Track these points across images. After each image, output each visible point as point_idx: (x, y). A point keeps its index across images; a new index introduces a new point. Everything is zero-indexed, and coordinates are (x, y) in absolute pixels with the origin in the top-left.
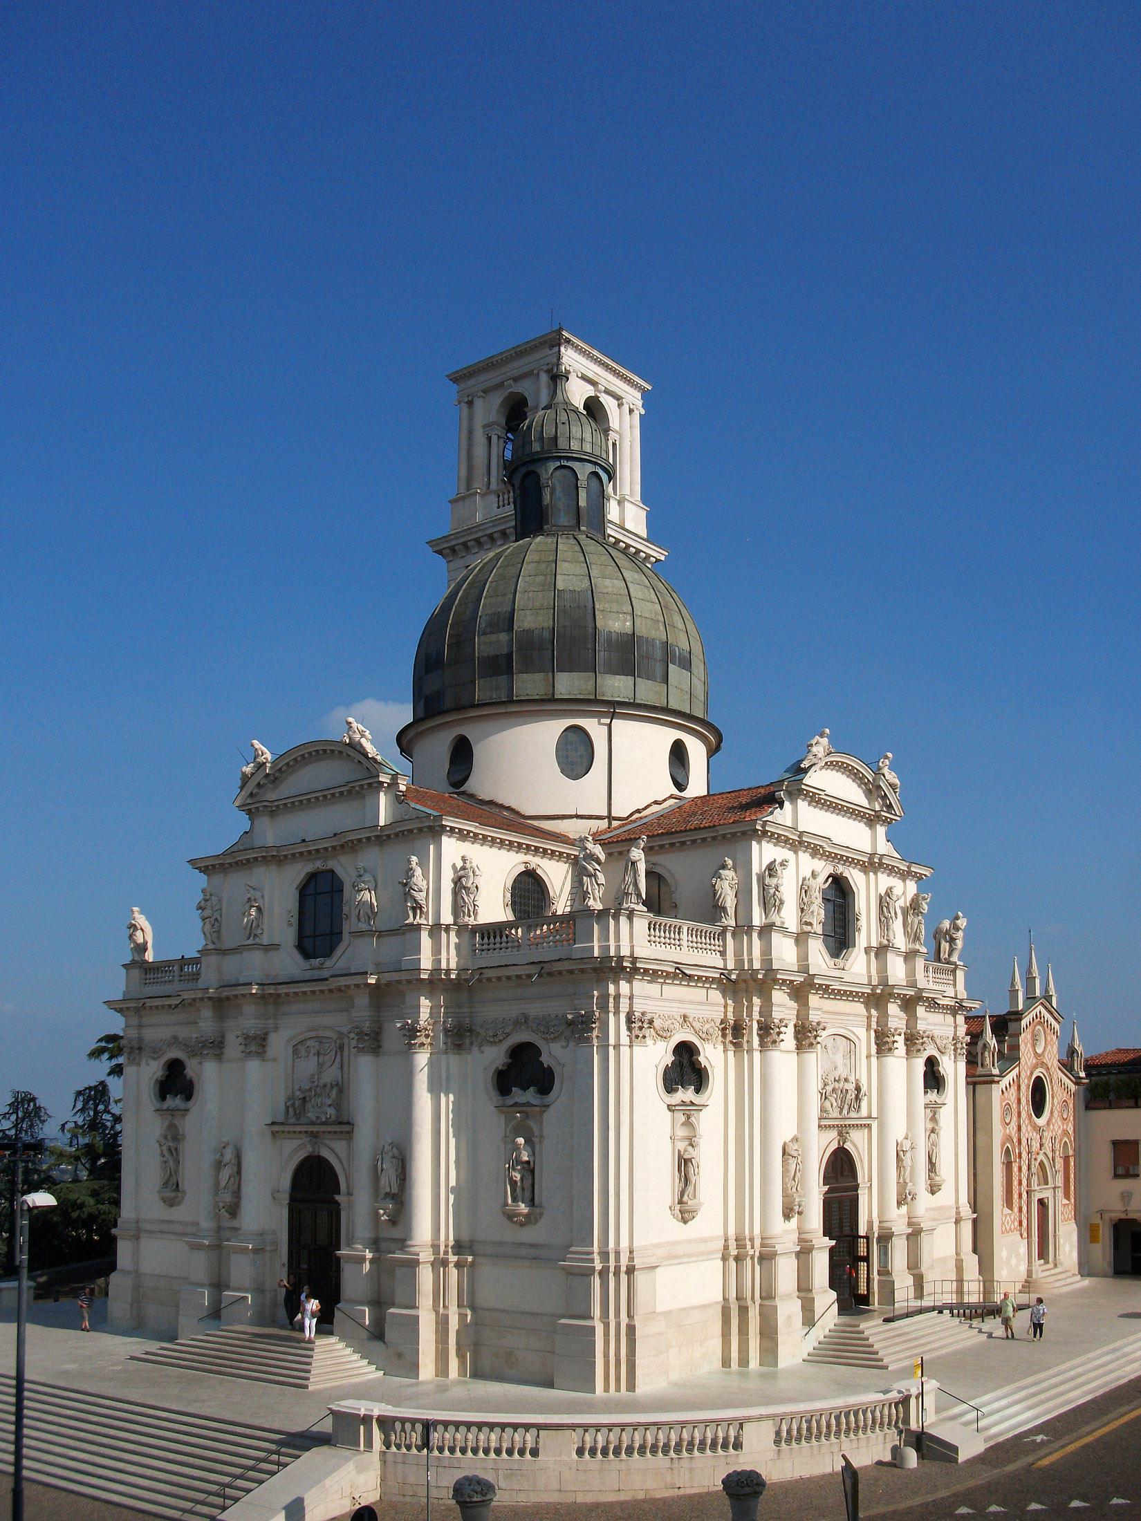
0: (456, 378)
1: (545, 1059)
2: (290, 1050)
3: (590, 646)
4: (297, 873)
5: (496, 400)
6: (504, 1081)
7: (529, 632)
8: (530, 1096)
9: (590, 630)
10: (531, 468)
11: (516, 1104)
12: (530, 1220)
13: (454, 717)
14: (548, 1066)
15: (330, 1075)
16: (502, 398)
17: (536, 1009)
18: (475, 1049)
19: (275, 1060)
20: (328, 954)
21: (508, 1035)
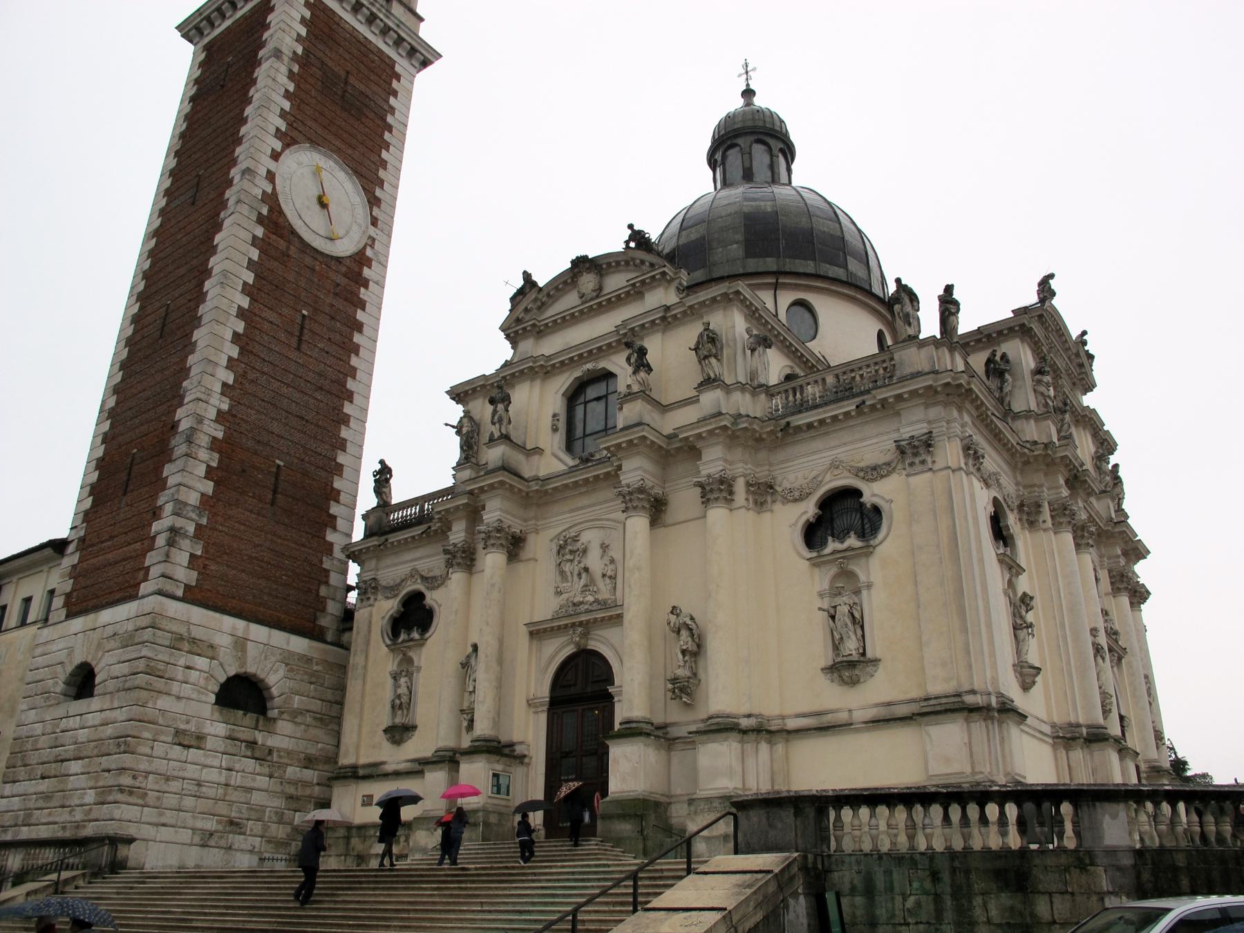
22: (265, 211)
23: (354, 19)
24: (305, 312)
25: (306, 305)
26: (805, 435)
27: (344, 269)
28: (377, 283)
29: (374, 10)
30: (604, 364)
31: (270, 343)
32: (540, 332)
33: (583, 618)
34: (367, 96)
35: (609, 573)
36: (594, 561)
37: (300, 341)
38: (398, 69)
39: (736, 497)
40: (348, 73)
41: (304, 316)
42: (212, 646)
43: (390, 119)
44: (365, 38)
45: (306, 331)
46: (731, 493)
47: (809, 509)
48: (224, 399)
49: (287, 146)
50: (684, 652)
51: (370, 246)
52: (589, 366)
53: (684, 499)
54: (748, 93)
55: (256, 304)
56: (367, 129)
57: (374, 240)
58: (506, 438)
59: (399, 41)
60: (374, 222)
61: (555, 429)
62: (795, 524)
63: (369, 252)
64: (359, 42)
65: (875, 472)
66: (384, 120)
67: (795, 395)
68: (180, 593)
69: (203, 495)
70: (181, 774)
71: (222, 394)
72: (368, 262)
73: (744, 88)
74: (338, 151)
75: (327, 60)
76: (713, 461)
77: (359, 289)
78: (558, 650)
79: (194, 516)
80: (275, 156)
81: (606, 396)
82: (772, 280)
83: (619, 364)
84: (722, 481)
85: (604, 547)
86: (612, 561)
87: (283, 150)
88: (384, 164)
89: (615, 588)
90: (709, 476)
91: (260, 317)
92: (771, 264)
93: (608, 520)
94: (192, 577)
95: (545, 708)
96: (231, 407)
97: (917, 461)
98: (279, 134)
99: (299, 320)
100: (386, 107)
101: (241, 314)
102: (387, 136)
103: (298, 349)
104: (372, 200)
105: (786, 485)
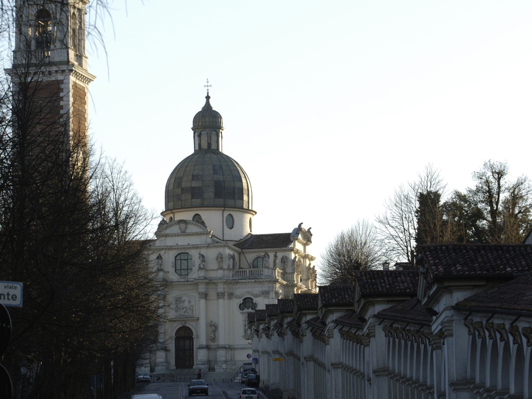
26: (242, 284)
30: (187, 251)
32: (167, 236)
33: (186, 319)
35: (192, 309)
36: (186, 304)
39: (225, 297)
46: (224, 295)
47: (241, 301)
50: (213, 330)
52: (183, 251)
53: (213, 294)
54: (208, 98)
58: (162, 270)
61: (173, 267)
62: (238, 304)
65: (257, 296)
67: (239, 272)
73: (206, 95)
76: (221, 288)
78: (177, 325)
81: (187, 260)
82: (223, 209)
83: (194, 254)
84: (223, 293)
85: (190, 302)
86: (192, 306)
89: (193, 312)
90: (220, 292)
92: (221, 201)
93: (191, 295)
95: (174, 339)
97: (266, 295)
105: (236, 294)
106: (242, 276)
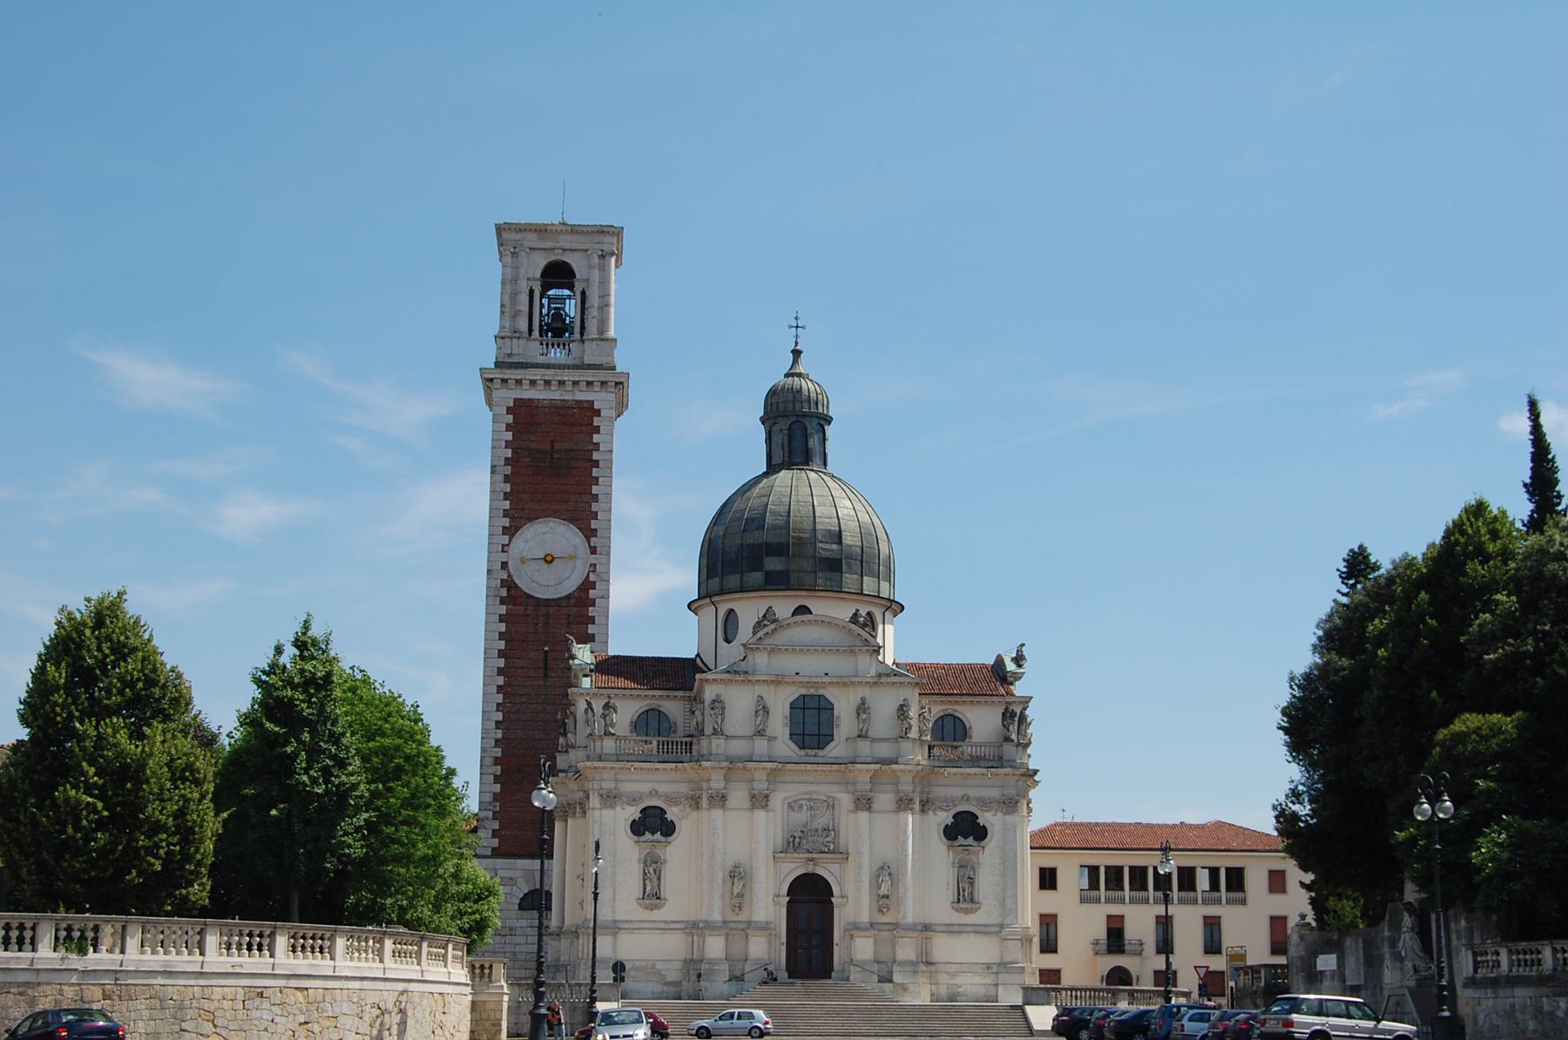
0: (500, 229)
1: (981, 821)
2: (786, 806)
3: (877, 561)
4: (789, 694)
5: (540, 262)
6: (951, 833)
7: (850, 546)
8: (970, 840)
9: (877, 551)
10: (800, 419)
11: (961, 845)
12: (967, 912)
13: (804, 593)
14: (984, 826)
15: (821, 822)
16: (544, 263)
17: (974, 793)
18: (931, 813)
19: (773, 811)
20: (820, 746)
21: (955, 806)
22: (504, 593)
23: (550, 392)
24: (546, 649)
25: (546, 643)
27: (572, 601)
28: (602, 597)
29: (559, 378)
31: (524, 681)
34: (572, 450)
37: (546, 669)
38: (596, 406)
40: (552, 442)
41: (547, 651)
42: (511, 878)
43: (596, 456)
44: (563, 400)
45: (549, 662)
48: (497, 731)
49: (512, 536)
51: (593, 571)
54: (797, 353)
55: (509, 661)
56: (576, 479)
57: (595, 565)
59: (589, 383)
60: (593, 551)
63: (592, 577)
64: (558, 408)
66: (592, 460)
68: (490, 853)
69: (494, 794)
70: (503, 950)
71: (497, 728)
72: (593, 585)
74: (556, 514)
75: (534, 445)
77: (588, 610)
79: (490, 807)
80: (504, 548)
87: (510, 542)
88: (595, 498)
91: (514, 668)
94: (495, 842)
96: (504, 734)
98: (505, 530)
99: (542, 656)
100: (591, 448)
101: (500, 671)
102: (595, 473)
103: (546, 675)
104: (589, 534)
106: (675, 754)
